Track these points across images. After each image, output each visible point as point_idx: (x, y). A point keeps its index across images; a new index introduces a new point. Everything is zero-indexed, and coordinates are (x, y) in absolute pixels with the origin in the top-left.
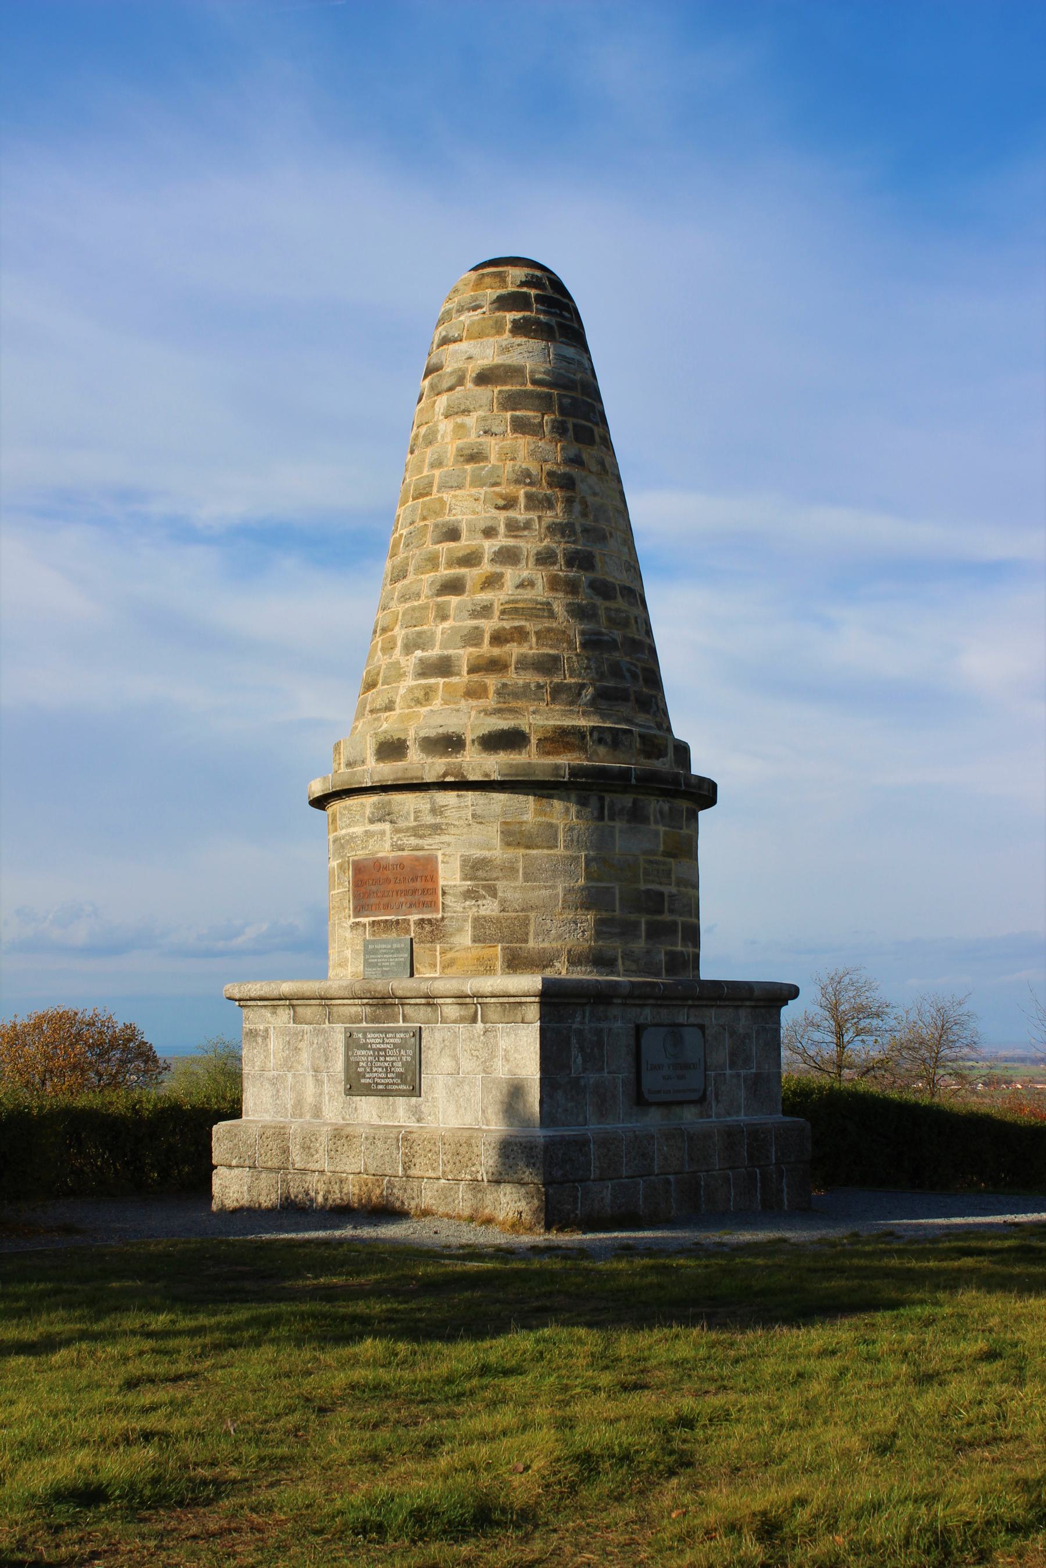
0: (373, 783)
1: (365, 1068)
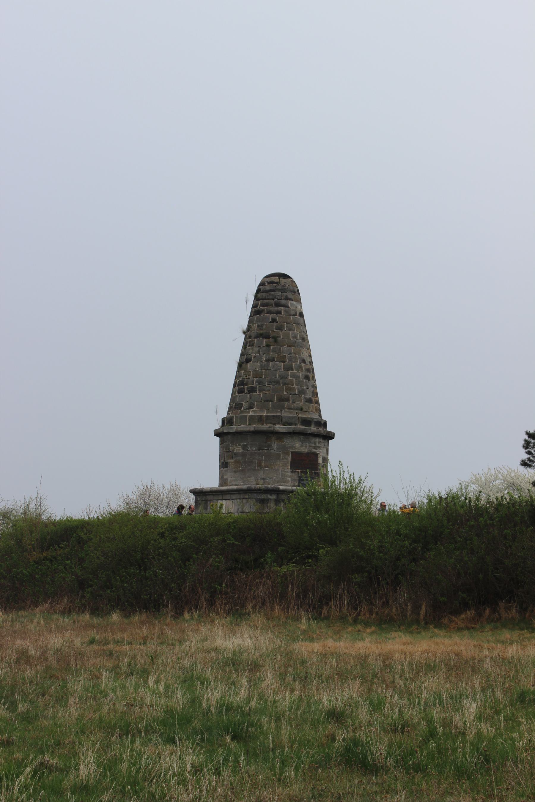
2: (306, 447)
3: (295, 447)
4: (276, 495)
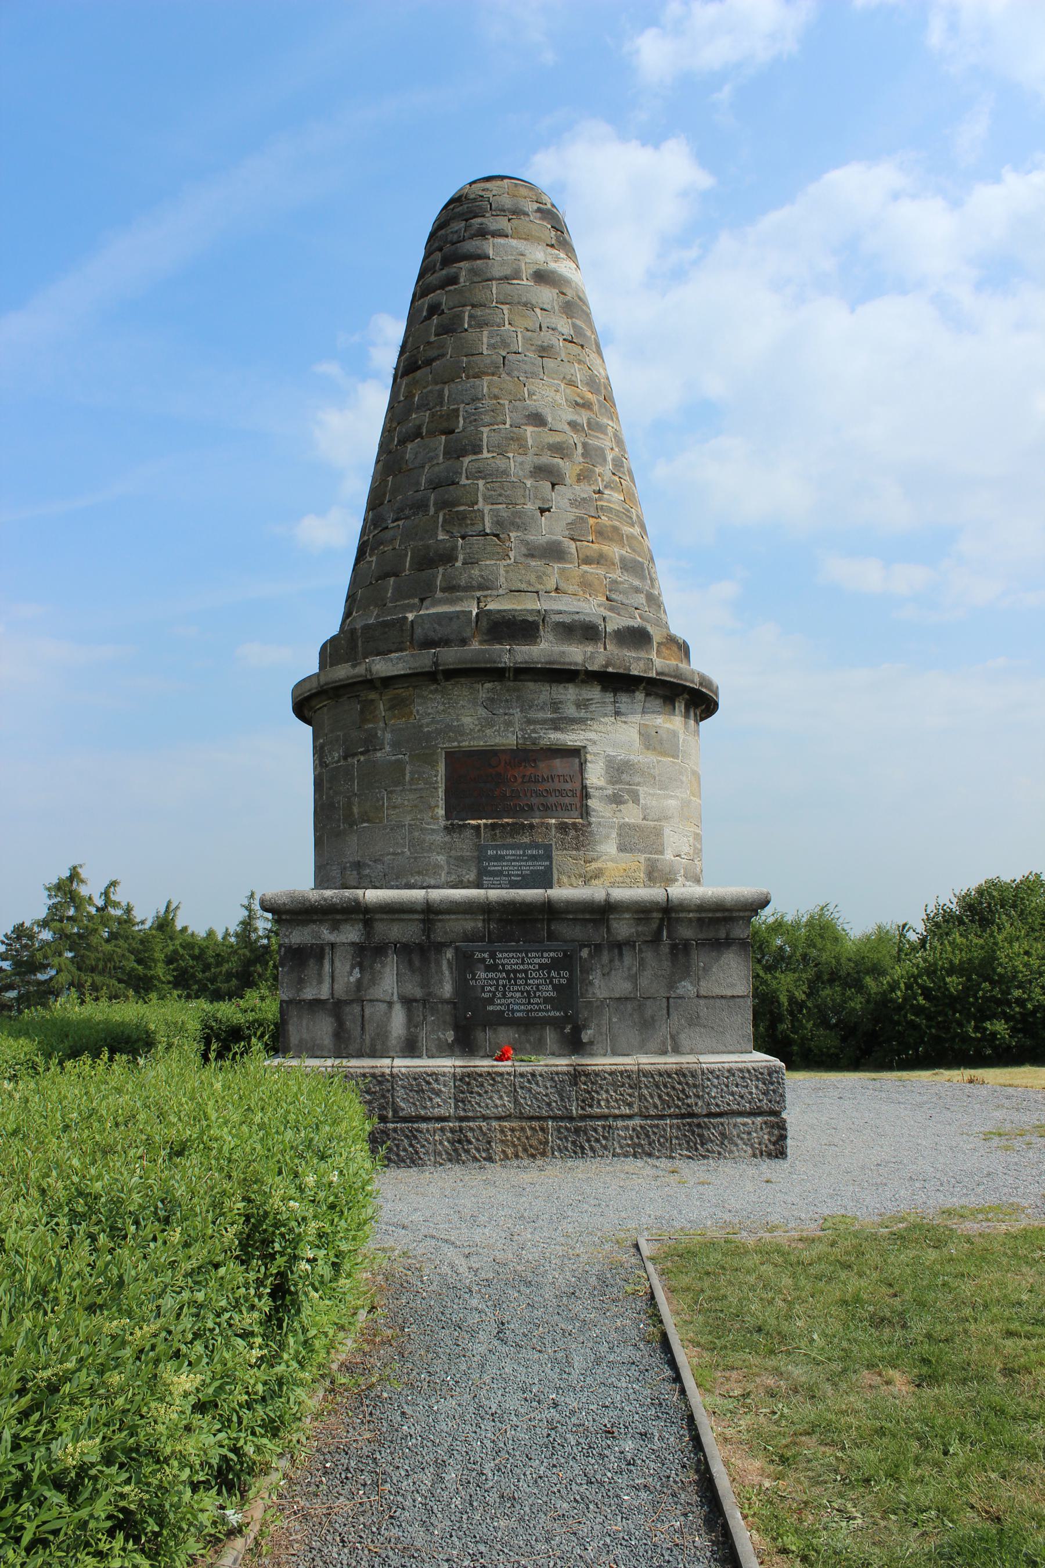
0: (515, 663)
1: (494, 993)
2: (509, 724)
3: (460, 731)
4: (361, 926)
